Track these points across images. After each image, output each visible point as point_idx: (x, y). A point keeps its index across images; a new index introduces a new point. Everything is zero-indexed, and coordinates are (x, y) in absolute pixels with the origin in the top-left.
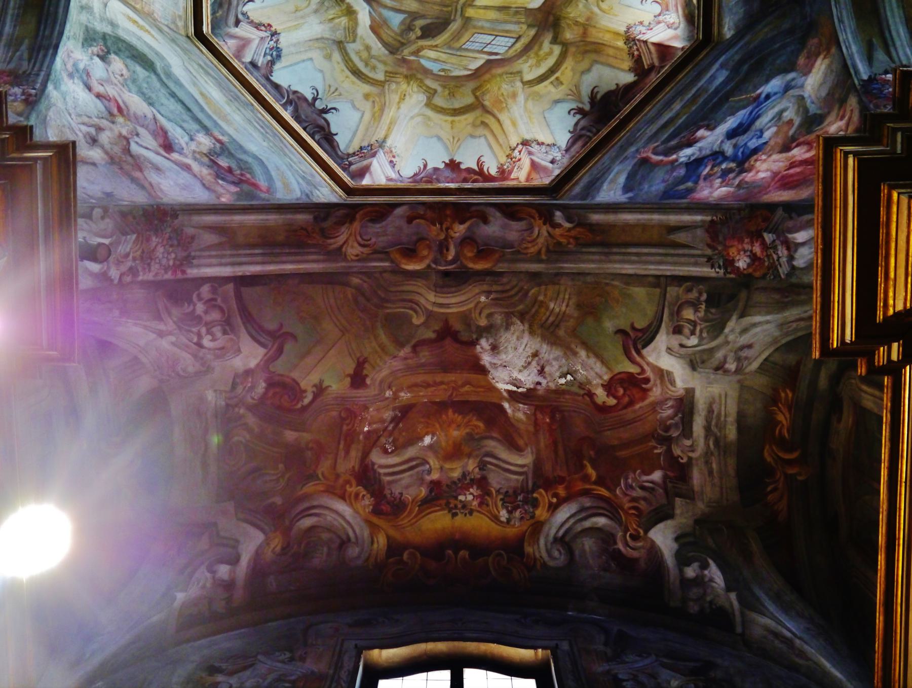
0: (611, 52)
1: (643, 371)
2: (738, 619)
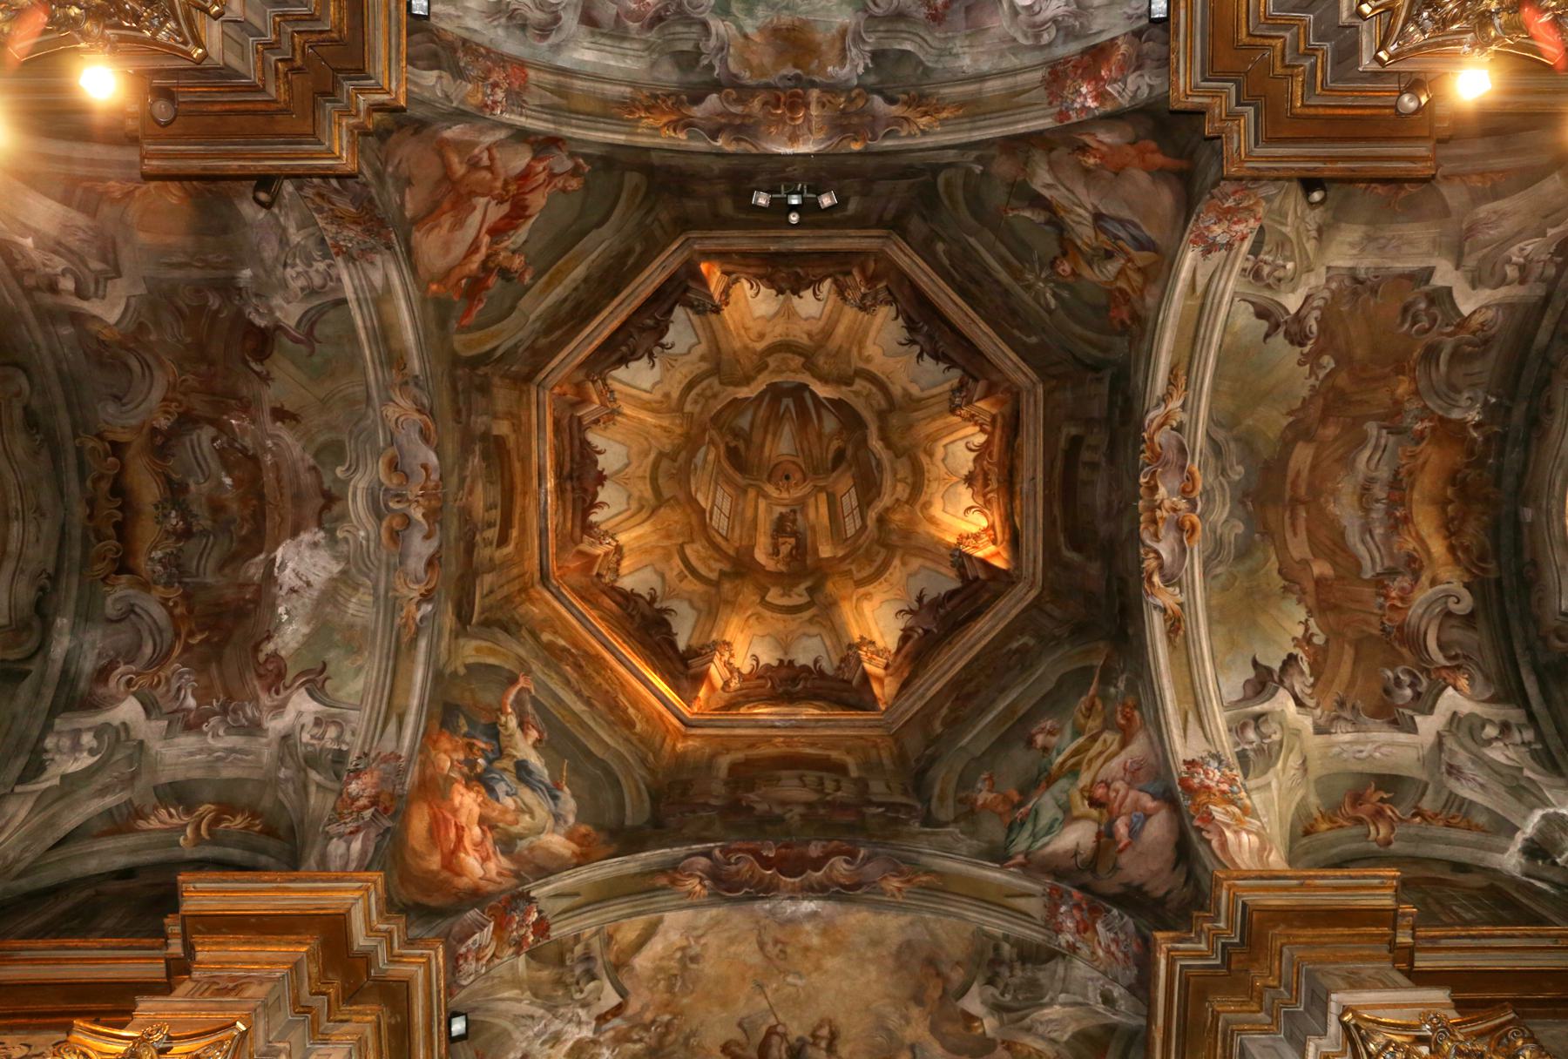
0: (708, 628)
1: (286, 688)
2: (30, 787)
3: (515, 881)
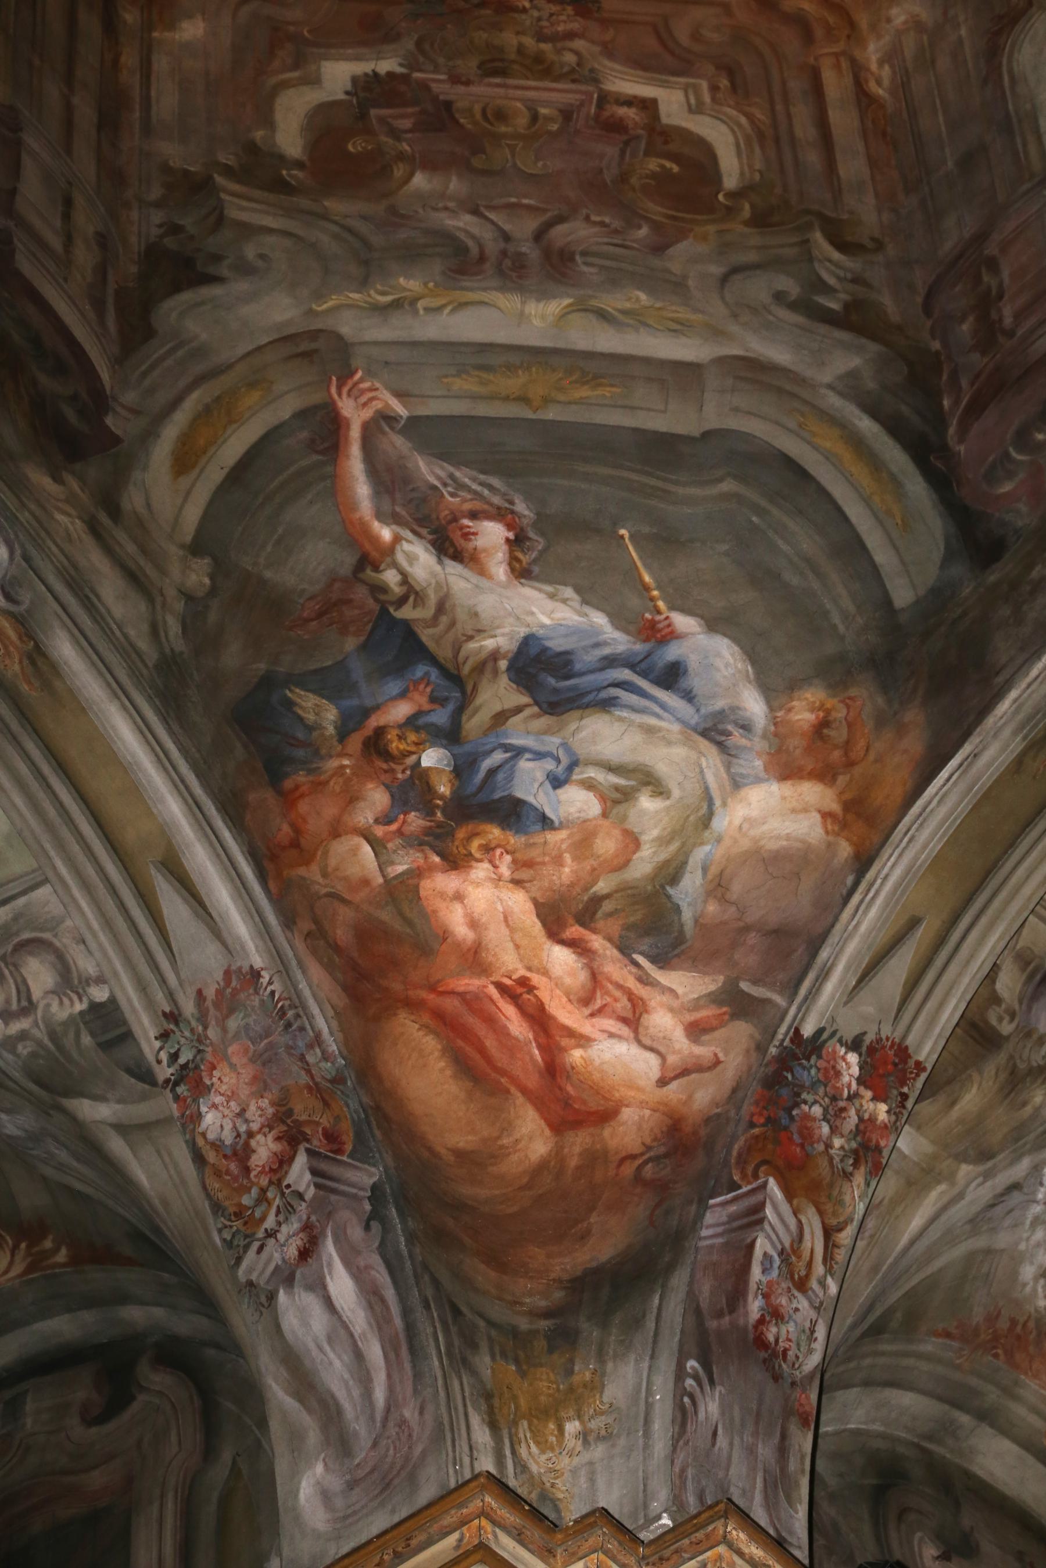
3: (742, 1032)
